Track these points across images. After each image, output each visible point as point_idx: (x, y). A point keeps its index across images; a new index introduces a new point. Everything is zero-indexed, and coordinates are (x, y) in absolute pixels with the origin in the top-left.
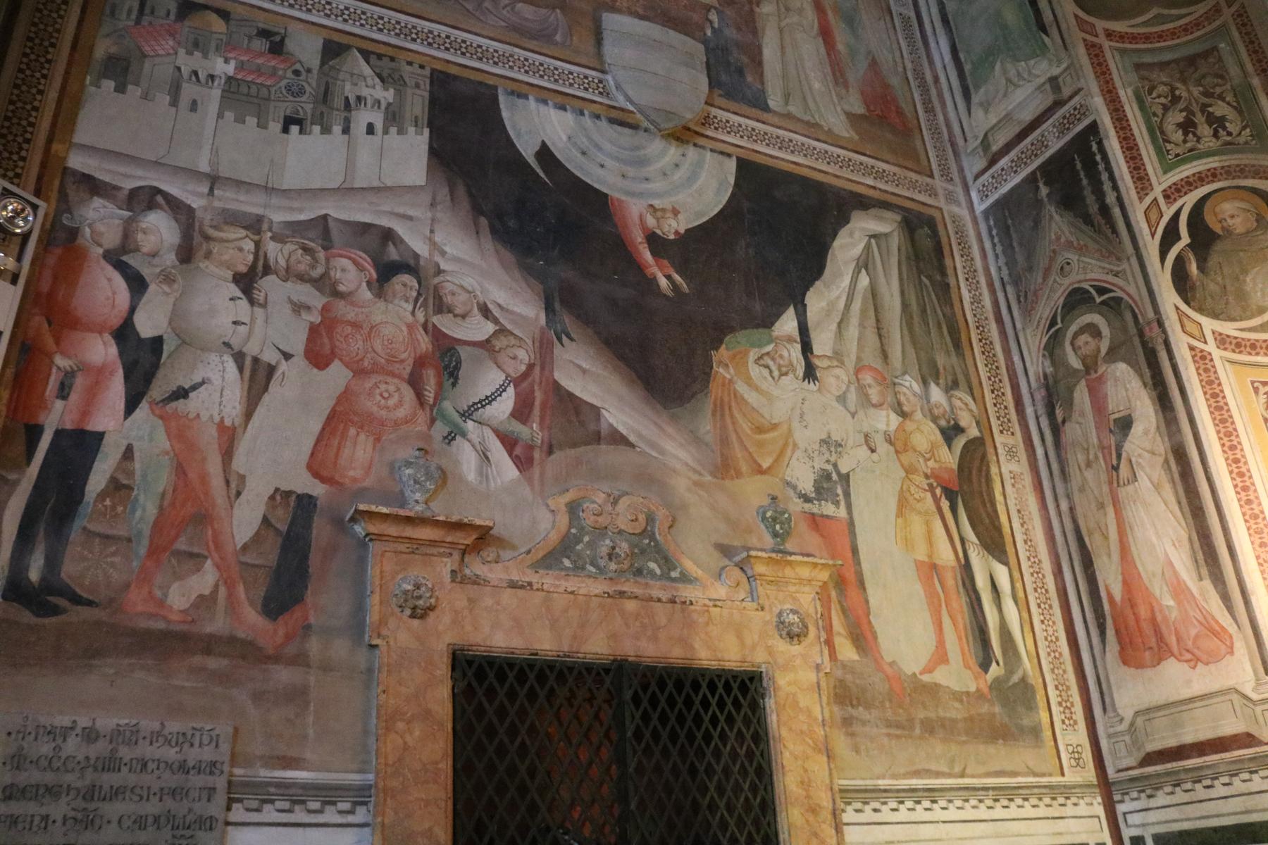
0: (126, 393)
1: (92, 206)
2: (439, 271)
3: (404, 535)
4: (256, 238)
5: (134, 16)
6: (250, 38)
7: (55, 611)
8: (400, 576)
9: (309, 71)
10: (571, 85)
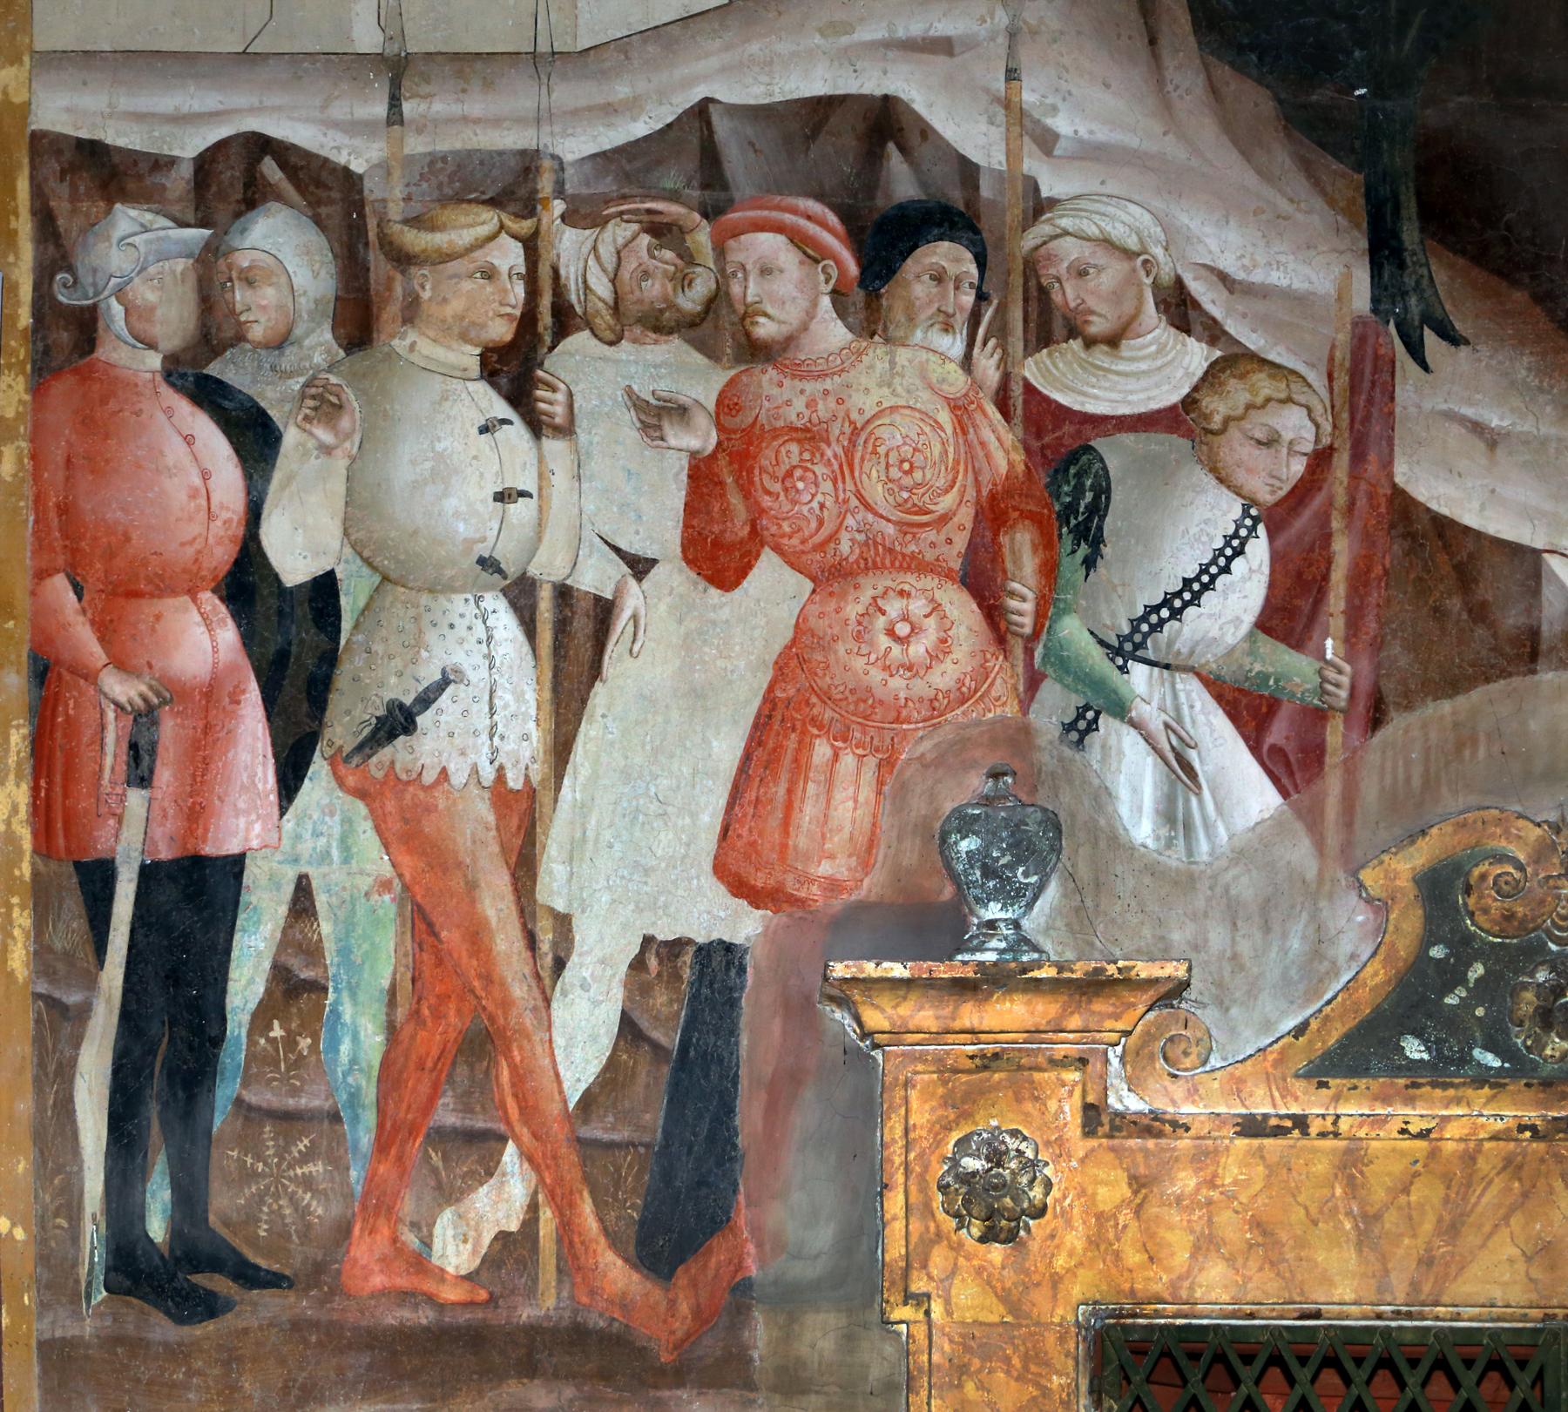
0: (273, 745)
1: (117, 234)
2: (1039, 207)
3: (957, 1025)
4: (526, 226)
8: (956, 1136)
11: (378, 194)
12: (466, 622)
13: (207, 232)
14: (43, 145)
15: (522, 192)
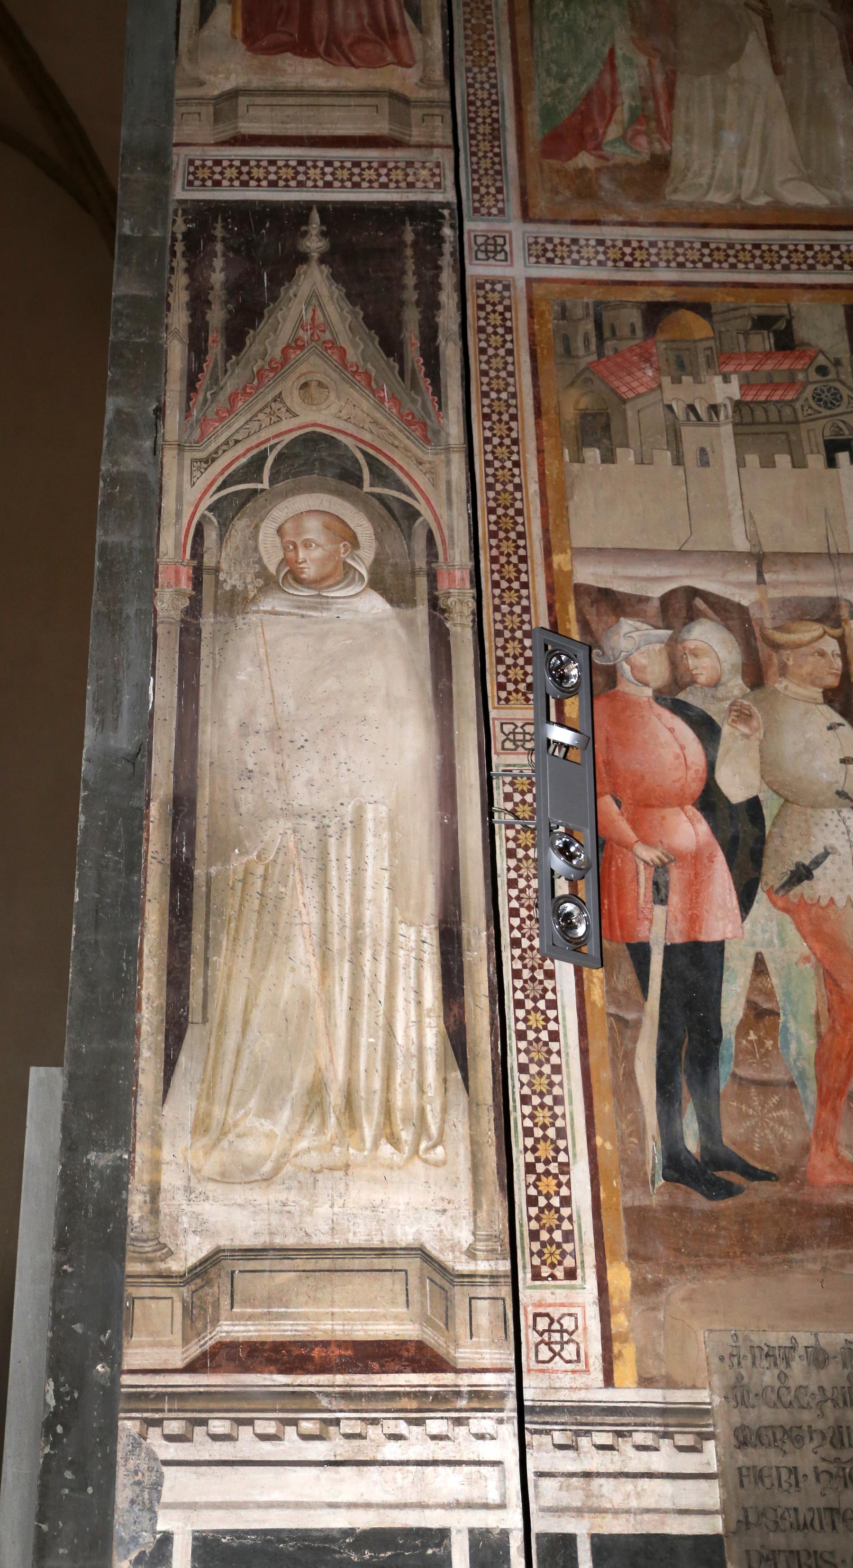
0: (735, 883)
5: (593, 347)
6: (746, 334)
7: (729, 1191)
9: (837, 363)
11: (758, 616)
12: (835, 823)
13: (670, 632)
14: (580, 590)
15: (833, 616)
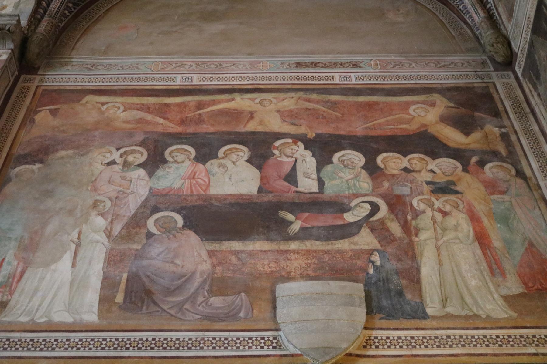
10: (250, 348)
